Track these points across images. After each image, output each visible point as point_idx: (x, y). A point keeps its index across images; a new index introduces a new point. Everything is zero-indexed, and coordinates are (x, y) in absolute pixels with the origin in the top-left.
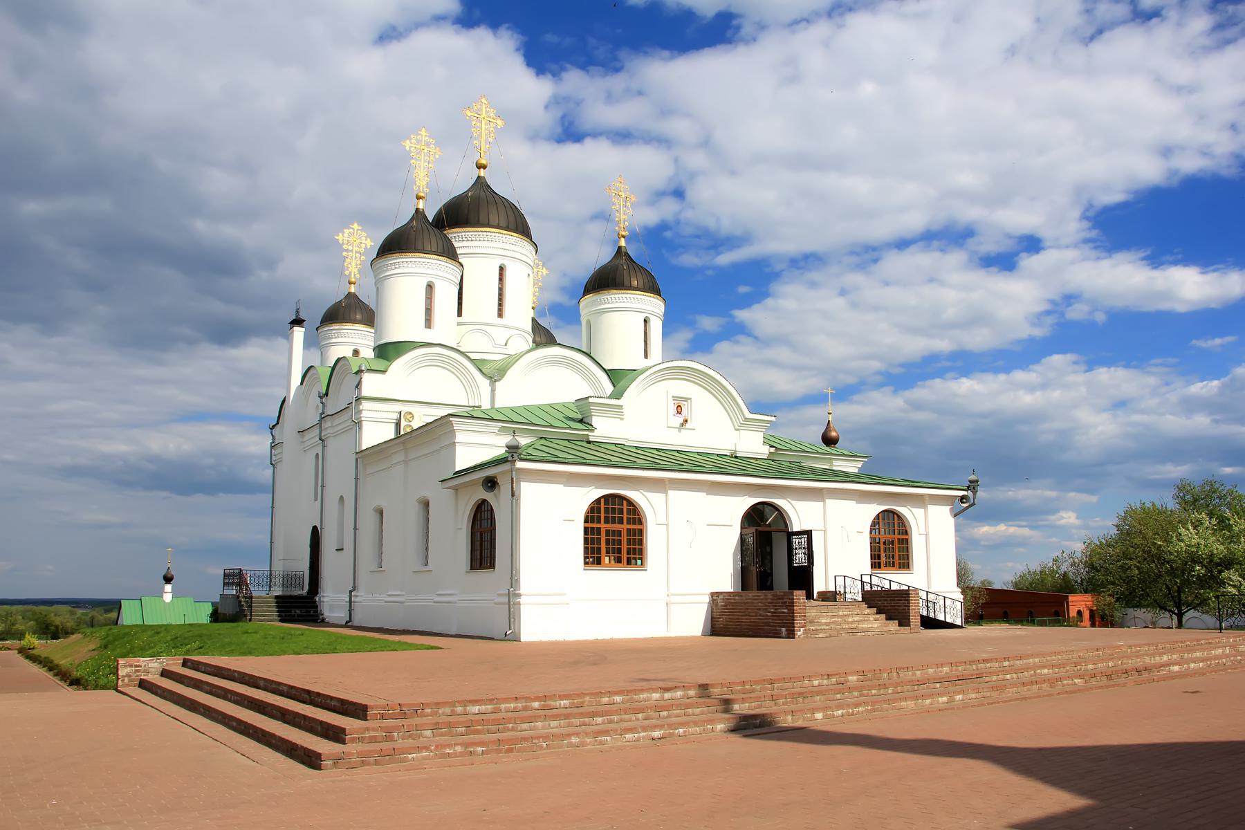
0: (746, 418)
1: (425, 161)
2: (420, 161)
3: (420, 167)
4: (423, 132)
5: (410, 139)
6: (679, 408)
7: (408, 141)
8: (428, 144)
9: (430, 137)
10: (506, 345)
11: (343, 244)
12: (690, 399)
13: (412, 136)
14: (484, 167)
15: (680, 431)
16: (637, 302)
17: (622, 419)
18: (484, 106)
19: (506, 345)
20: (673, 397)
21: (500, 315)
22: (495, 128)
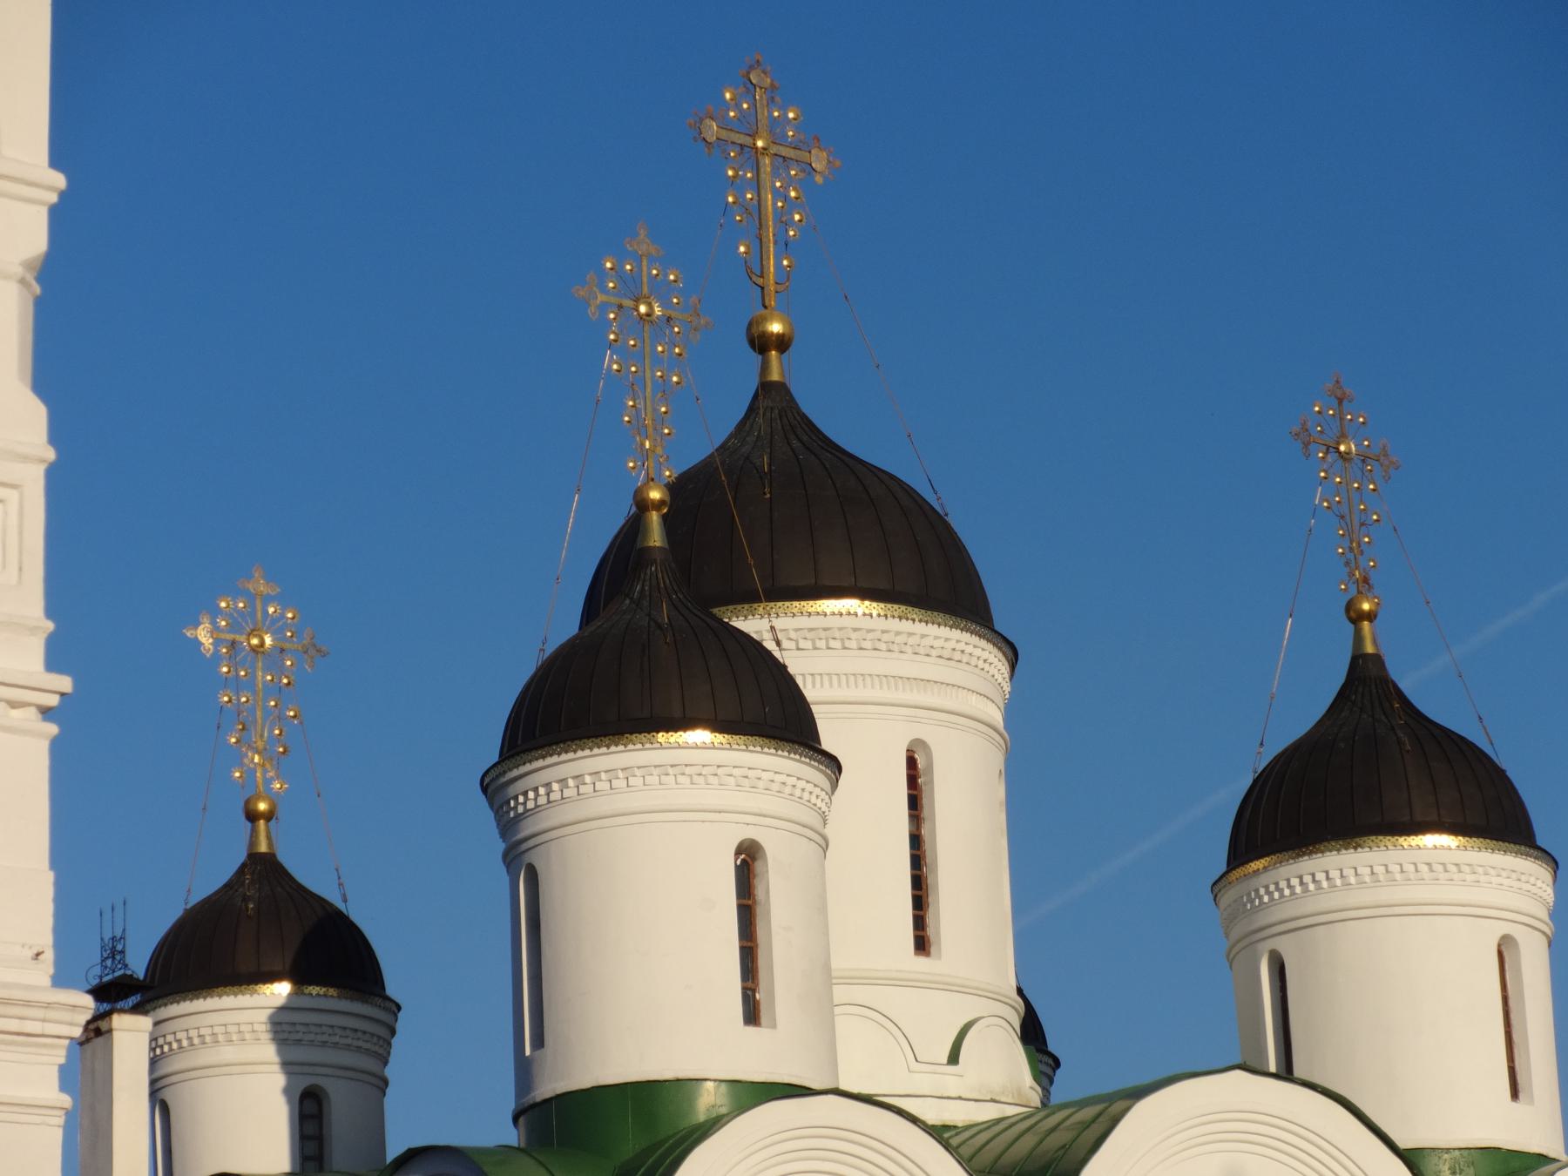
5: (602, 275)
10: (954, 1058)
11: (216, 659)
14: (782, 343)
16: (1442, 875)
19: (954, 1058)
21: (922, 945)
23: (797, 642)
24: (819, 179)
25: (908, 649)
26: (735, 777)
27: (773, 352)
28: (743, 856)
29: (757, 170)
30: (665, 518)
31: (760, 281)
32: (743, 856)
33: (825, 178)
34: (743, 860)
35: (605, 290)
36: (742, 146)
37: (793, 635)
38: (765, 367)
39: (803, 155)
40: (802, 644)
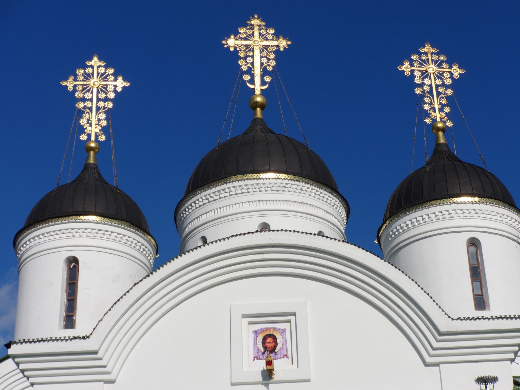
0: (441, 334)
1: (98, 100)
2: (91, 100)
3: (91, 109)
4: (95, 61)
6: (269, 340)
7: (71, 78)
8: (104, 77)
9: (106, 67)
12: (294, 314)
13: (80, 72)
15: (267, 385)
17: (107, 382)
18: (256, 29)
20: (245, 316)
22: (277, 52)
23: (214, 197)
24: (282, 49)
25: (257, 190)
26: (66, 233)
27: (258, 109)
28: (74, 264)
29: (253, 51)
30: (96, 153)
31: (252, 86)
32: (74, 264)
33: (285, 48)
34: (74, 266)
35: (75, 80)
36: (246, 46)
37: (212, 195)
38: (255, 114)
39: (275, 43)
40: (216, 198)
